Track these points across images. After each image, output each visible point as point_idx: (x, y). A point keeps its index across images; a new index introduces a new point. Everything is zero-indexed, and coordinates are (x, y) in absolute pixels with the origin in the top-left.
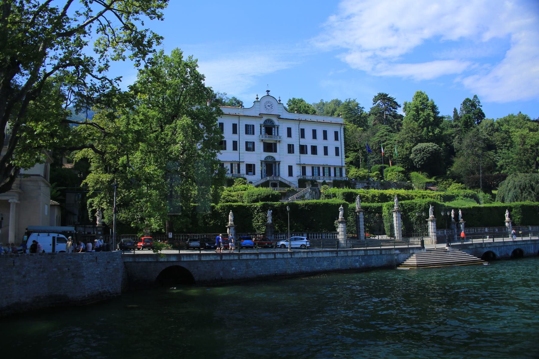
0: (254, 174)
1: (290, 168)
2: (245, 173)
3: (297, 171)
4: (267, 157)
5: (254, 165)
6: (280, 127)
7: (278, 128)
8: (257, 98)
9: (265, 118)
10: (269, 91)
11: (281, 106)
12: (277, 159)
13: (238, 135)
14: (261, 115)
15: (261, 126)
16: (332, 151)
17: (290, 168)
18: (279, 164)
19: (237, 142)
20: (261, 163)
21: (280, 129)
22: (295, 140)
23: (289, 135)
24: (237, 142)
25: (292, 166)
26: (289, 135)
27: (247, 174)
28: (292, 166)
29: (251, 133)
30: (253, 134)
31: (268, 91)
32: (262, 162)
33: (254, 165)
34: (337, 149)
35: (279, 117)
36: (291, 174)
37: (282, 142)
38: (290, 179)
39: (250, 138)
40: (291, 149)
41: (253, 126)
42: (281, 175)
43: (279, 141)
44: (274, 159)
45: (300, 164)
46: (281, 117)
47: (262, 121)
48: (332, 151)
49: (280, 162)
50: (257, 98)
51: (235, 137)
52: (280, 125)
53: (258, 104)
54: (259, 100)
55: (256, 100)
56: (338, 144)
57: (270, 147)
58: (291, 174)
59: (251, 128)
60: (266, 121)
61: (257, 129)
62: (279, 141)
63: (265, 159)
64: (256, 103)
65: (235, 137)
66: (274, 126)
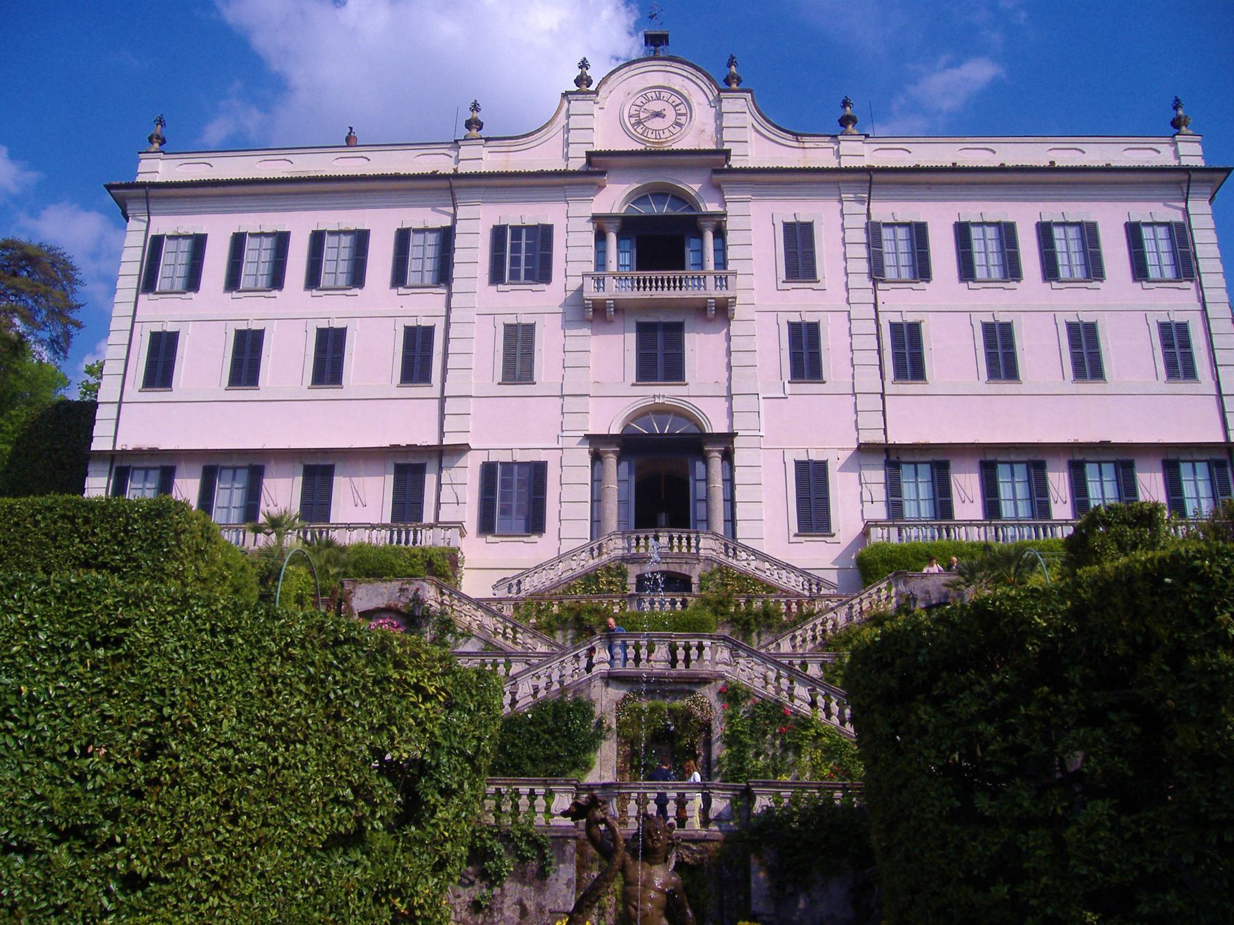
2: (470, 515)
4: (640, 415)
6: (730, 224)
7: (720, 234)
8: (582, 80)
15: (600, 237)
18: (728, 456)
19: (428, 332)
20: (597, 458)
21: (731, 238)
24: (428, 332)
25: (821, 467)
27: (486, 526)
28: (821, 467)
37: (739, 312)
42: (744, 532)
44: (698, 424)
46: (735, 163)
49: (729, 437)
52: (731, 208)
54: (592, 88)
55: (575, 88)
60: (639, 197)
63: (626, 426)
64: (577, 106)
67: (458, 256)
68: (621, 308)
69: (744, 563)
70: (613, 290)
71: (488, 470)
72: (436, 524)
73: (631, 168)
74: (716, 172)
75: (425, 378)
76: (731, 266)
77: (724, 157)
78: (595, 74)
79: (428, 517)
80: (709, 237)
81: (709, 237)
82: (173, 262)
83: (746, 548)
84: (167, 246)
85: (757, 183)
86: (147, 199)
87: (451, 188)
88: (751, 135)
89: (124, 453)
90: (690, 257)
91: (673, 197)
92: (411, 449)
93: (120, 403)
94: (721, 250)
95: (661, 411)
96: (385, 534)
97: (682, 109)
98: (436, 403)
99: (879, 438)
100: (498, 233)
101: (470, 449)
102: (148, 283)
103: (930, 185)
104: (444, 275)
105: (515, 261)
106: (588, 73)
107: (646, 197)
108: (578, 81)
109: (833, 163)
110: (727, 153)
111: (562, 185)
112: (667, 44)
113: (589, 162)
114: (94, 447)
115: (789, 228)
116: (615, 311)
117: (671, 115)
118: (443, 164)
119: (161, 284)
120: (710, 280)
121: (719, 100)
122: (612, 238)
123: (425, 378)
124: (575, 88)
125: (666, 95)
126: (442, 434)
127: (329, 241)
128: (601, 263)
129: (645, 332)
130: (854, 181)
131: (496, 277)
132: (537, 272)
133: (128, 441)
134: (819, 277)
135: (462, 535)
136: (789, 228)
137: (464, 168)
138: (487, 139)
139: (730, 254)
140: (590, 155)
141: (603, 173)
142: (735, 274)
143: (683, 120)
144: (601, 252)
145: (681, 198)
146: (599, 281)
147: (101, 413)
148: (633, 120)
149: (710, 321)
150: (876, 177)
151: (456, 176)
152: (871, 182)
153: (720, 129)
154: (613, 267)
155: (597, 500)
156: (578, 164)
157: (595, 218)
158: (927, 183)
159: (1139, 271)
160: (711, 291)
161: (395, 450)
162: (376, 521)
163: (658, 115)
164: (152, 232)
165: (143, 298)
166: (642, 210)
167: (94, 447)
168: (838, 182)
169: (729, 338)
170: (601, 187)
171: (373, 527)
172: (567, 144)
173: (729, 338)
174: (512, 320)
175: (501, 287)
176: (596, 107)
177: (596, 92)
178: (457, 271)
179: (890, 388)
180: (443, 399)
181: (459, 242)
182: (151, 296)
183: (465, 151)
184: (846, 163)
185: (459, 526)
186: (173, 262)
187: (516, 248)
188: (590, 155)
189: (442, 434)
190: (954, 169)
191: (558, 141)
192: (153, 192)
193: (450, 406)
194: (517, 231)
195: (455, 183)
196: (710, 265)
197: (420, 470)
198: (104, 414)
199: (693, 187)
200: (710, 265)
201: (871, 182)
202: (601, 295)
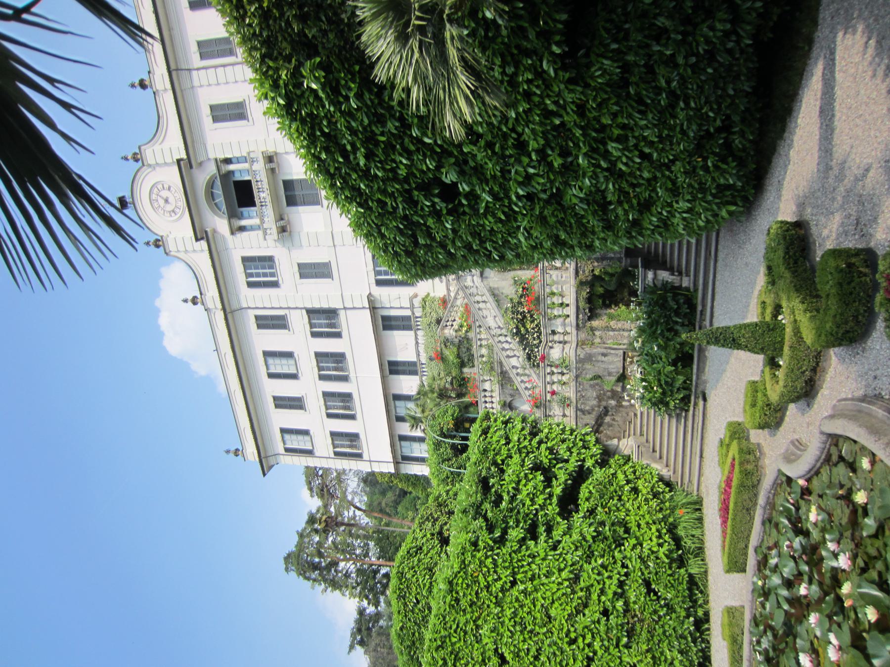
6: (222, 156)
7: (228, 161)
11: (149, 154)
13: (287, 311)
15: (242, 229)
21: (229, 156)
29: (271, 267)
35: (186, 166)
37: (271, 149)
39: (286, 270)
43: (270, 159)
47: (220, 224)
52: (212, 156)
62: (270, 159)
64: (171, 247)
65: (299, 321)
71: (379, 283)
72: (412, 307)
73: (200, 215)
74: (191, 167)
76: (245, 154)
77: (182, 163)
78: (152, 239)
80: (232, 167)
81: (232, 167)
82: (295, 442)
84: (288, 446)
85: (193, 142)
86: (266, 457)
87: (232, 312)
88: (166, 145)
89: (394, 457)
90: (247, 178)
91: (212, 188)
93: (370, 461)
94: (238, 160)
96: (420, 333)
97: (160, 186)
98: (348, 312)
100: (251, 285)
101: (370, 294)
102: (309, 453)
103: (170, 29)
105: (265, 275)
106: (152, 241)
107: (216, 204)
108: (158, 246)
109: (171, 92)
110: (179, 161)
111: (218, 253)
112: (123, 197)
113: (202, 239)
114: (393, 471)
115: (216, 119)
116: (282, 219)
117: (165, 194)
118: (220, 316)
119: (309, 447)
120: (256, 167)
121: (149, 166)
122: (243, 223)
124: (162, 248)
125: (154, 197)
126: (364, 308)
127: (273, 370)
129: (291, 201)
130: (179, 80)
131: (275, 284)
132: (270, 263)
134: (240, 100)
135: (416, 296)
136: (216, 119)
137: (220, 306)
138: (201, 294)
139: (238, 155)
140: (197, 240)
141: (206, 232)
142: (249, 153)
143: (166, 186)
144: (252, 228)
145: (211, 185)
148: (173, 214)
150: (173, 66)
151: (224, 309)
152: (177, 70)
153: (166, 164)
156: (204, 243)
157: (232, 233)
158: (170, 30)
162: (414, 342)
163: (166, 201)
164: (283, 452)
165: (317, 454)
166: (224, 207)
167: (393, 471)
168: (182, 91)
169: (286, 153)
170: (214, 231)
171: (417, 343)
172: (194, 251)
173: (286, 153)
174: (297, 275)
175: (280, 282)
176: (171, 237)
177: (162, 237)
180: (345, 308)
182: (315, 451)
183: (210, 305)
184: (168, 86)
186: (295, 442)
187: (258, 275)
188: (197, 240)
189: (364, 308)
190: (156, 12)
191: (193, 255)
192: (262, 455)
193: (348, 305)
194: (249, 275)
195: (228, 310)
197: (385, 319)
198: (377, 468)
201: (177, 70)
202: (274, 230)
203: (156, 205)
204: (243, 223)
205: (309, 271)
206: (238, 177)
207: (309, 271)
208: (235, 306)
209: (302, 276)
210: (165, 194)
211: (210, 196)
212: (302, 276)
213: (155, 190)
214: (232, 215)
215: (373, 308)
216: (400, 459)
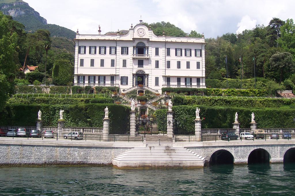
0: (127, 84)
1: (157, 79)
3: (162, 83)
5: (127, 77)
8: (132, 27)
9: (137, 42)
10: (142, 21)
12: (146, 73)
14: (134, 39)
16: (193, 65)
17: (157, 79)
18: (148, 76)
22: (162, 57)
23: (157, 53)
26: (157, 53)
27: (122, 84)
29: (125, 53)
30: (127, 54)
31: (141, 21)
32: (133, 75)
33: (127, 77)
34: (198, 64)
36: (157, 84)
38: (156, 88)
39: (125, 57)
40: (157, 65)
41: (128, 48)
45: (165, 76)
46: (150, 40)
48: (193, 65)
50: (132, 27)
51: (113, 57)
53: (133, 31)
54: (133, 28)
56: (199, 59)
57: (141, 63)
58: (157, 84)
59: (126, 50)
60: (138, 43)
61: (131, 49)
62: (148, 59)
66: (145, 47)
67: (117, 51)
68: (136, 58)
69: (149, 90)
70: (135, 57)
75: (114, 66)
79: (115, 83)
80: (146, 48)
83: (149, 88)
92: (112, 75)
94: (148, 51)
95: (141, 71)
99: (164, 75)
104: (116, 53)
117: (142, 32)
119: (81, 53)
120: (146, 56)
122: (135, 49)
123: (114, 66)
124: (131, 28)
125: (142, 29)
128: (134, 53)
131: (122, 53)
133: (79, 73)
140: (133, 39)
143: (144, 33)
145: (143, 43)
146: (134, 55)
147: (75, 69)
149: (147, 60)
154: (135, 53)
155: (133, 80)
156: (132, 40)
159: (196, 55)
160: (146, 57)
161: (111, 75)
163: (141, 32)
178: (117, 52)
179: (166, 69)
181: (117, 49)
185: (119, 84)
188: (133, 39)
196: (146, 54)
199: (145, 42)
200: (146, 54)
202: (134, 57)
203: (140, 29)
204: (135, 49)
205: (125, 62)
206: (145, 49)
207: (125, 62)
208: (118, 43)
209: (124, 60)
210: (142, 32)
211: (141, 42)
212: (124, 60)
213: (143, 30)
214: (137, 47)
215: (116, 75)
216: (79, 76)
